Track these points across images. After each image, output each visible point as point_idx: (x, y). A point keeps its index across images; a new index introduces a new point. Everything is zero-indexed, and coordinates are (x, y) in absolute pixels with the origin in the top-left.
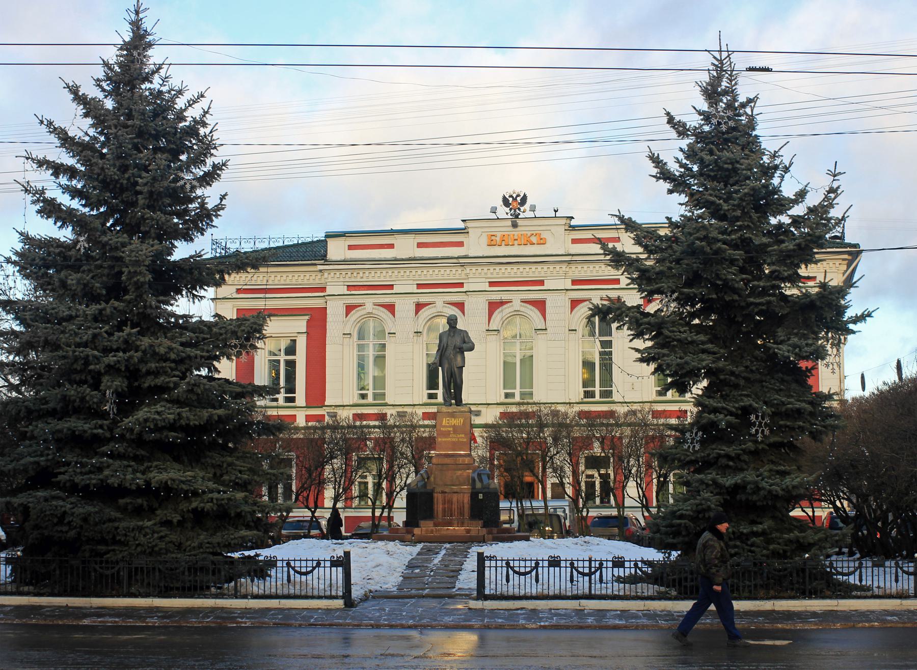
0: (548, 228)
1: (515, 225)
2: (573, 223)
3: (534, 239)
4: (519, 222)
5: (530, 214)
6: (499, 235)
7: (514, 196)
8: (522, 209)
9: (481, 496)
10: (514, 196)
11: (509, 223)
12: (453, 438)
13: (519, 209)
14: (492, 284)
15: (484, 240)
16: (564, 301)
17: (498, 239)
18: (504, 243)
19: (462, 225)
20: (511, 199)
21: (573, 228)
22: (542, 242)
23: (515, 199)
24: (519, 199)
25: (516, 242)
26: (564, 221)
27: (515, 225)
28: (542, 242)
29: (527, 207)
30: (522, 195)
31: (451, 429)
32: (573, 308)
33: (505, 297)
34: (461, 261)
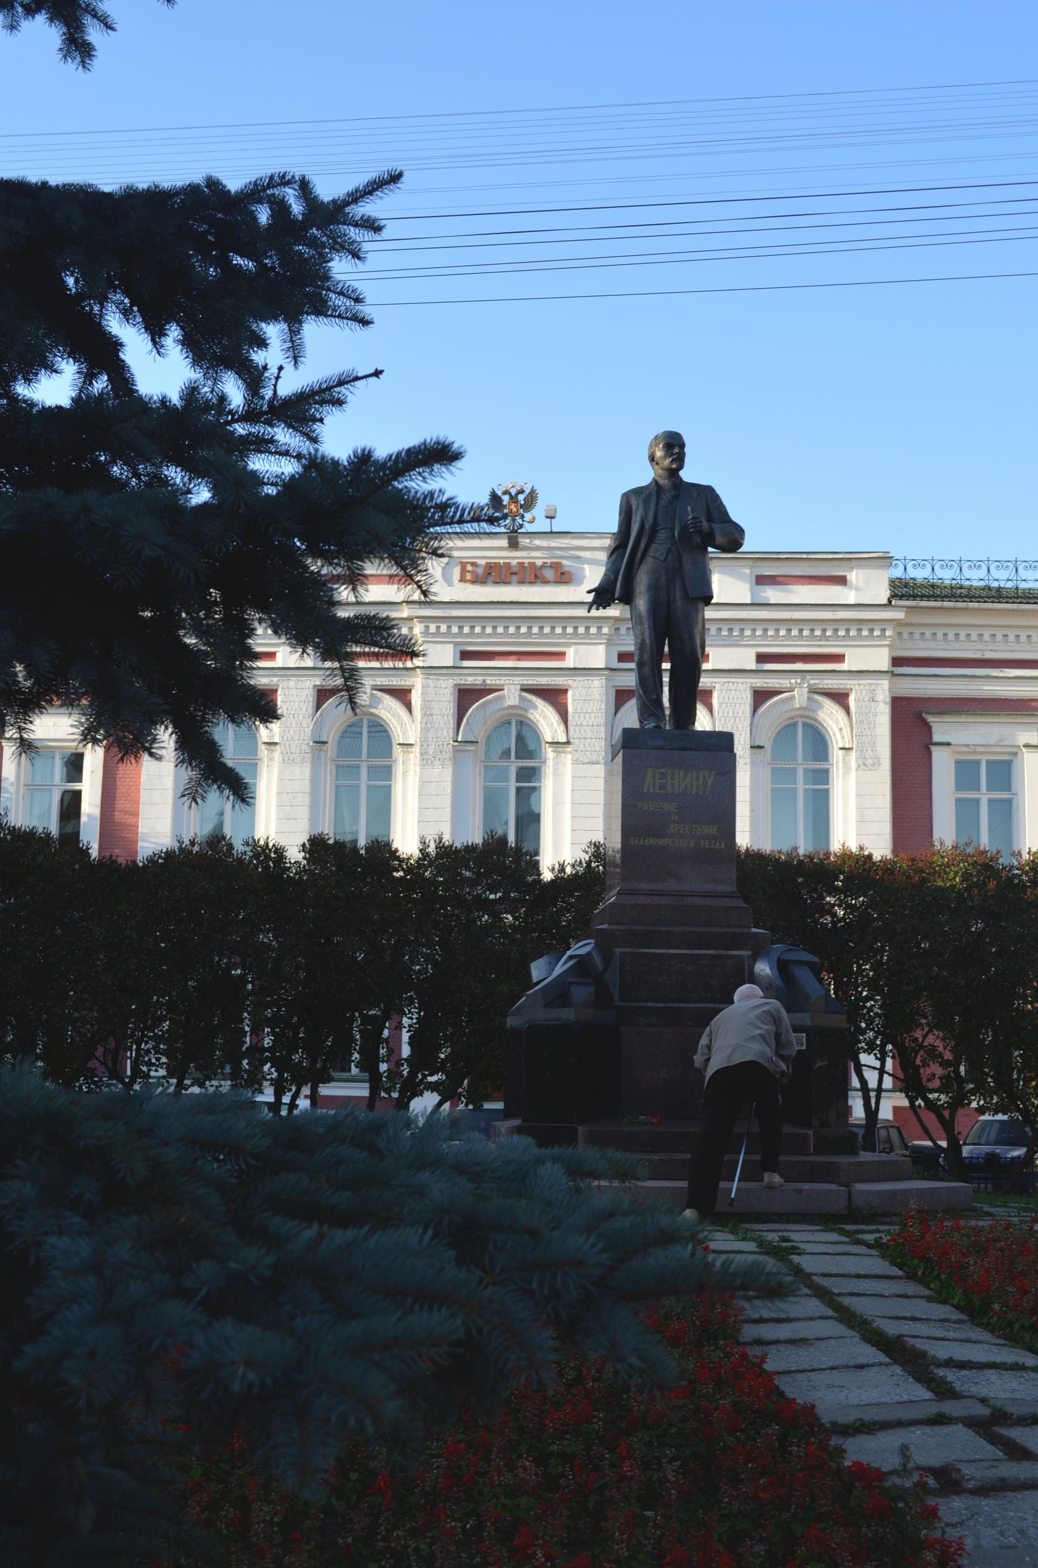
1: (514, 544)
3: (549, 574)
4: (524, 541)
5: (542, 525)
7: (513, 492)
8: (528, 516)
10: (513, 492)
11: (504, 542)
13: (523, 517)
18: (491, 579)
20: (506, 499)
23: (513, 499)
24: (521, 497)
25: (515, 578)
29: (538, 511)
30: (527, 492)
33: (491, 681)
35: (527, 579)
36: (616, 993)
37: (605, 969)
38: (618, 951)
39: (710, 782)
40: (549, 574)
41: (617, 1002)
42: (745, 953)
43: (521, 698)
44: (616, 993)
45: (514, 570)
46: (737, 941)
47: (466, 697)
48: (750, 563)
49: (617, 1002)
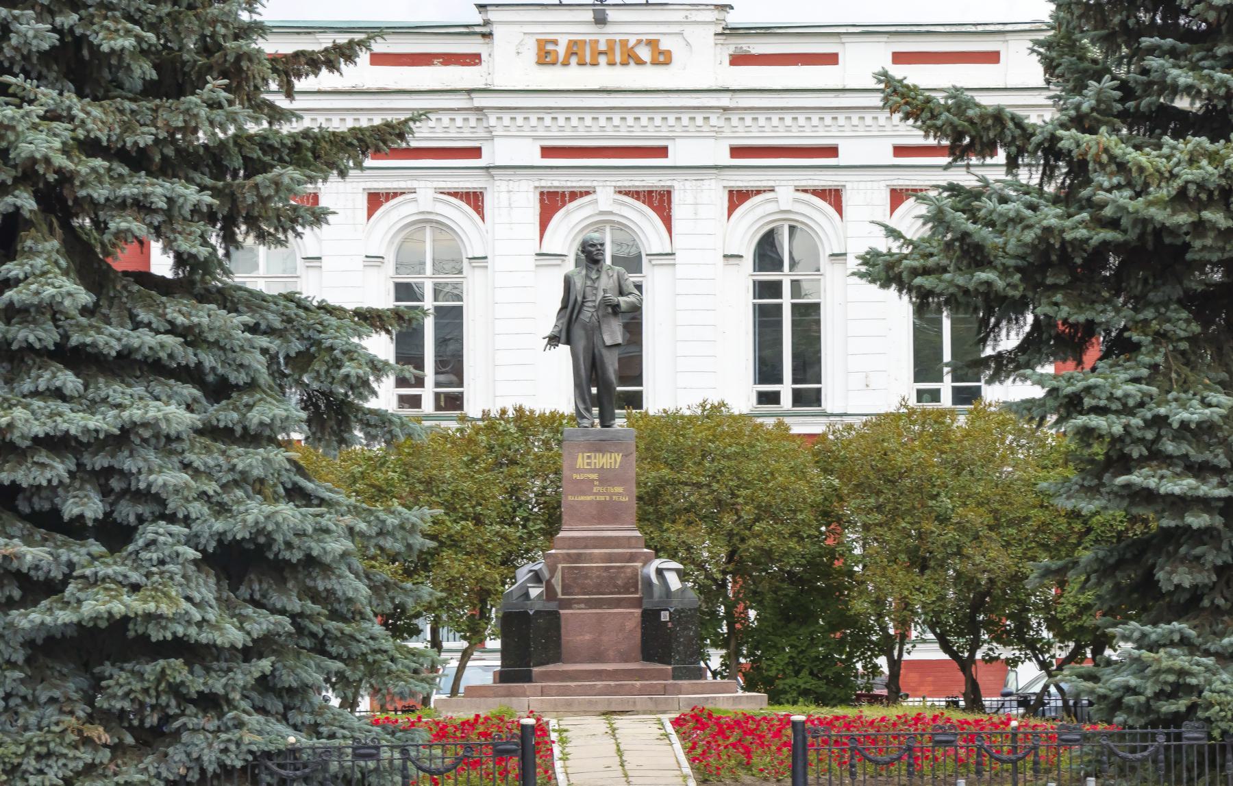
0: (676, 29)
2: (733, 19)
3: (644, 53)
4: (612, 15)
6: (563, 42)
9: (665, 617)
11: (589, 15)
12: (598, 495)
14: (547, 152)
15: (531, 53)
16: (714, 193)
17: (561, 50)
18: (574, 60)
19: (477, 18)
21: (732, 32)
22: (662, 58)
26: (711, 15)
27: (601, 20)
28: (662, 58)
31: (594, 476)
32: (732, 208)
34: (480, 101)
35: (618, 59)
36: (559, 590)
37: (552, 577)
38: (560, 566)
39: (619, 460)
40: (644, 53)
41: (560, 596)
42: (639, 564)
43: (615, 201)
44: (559, 590)
45: (602, 47)
46: (632, 558)
47: (551, 203)
48: (884, 38)
49: (560, 596)
